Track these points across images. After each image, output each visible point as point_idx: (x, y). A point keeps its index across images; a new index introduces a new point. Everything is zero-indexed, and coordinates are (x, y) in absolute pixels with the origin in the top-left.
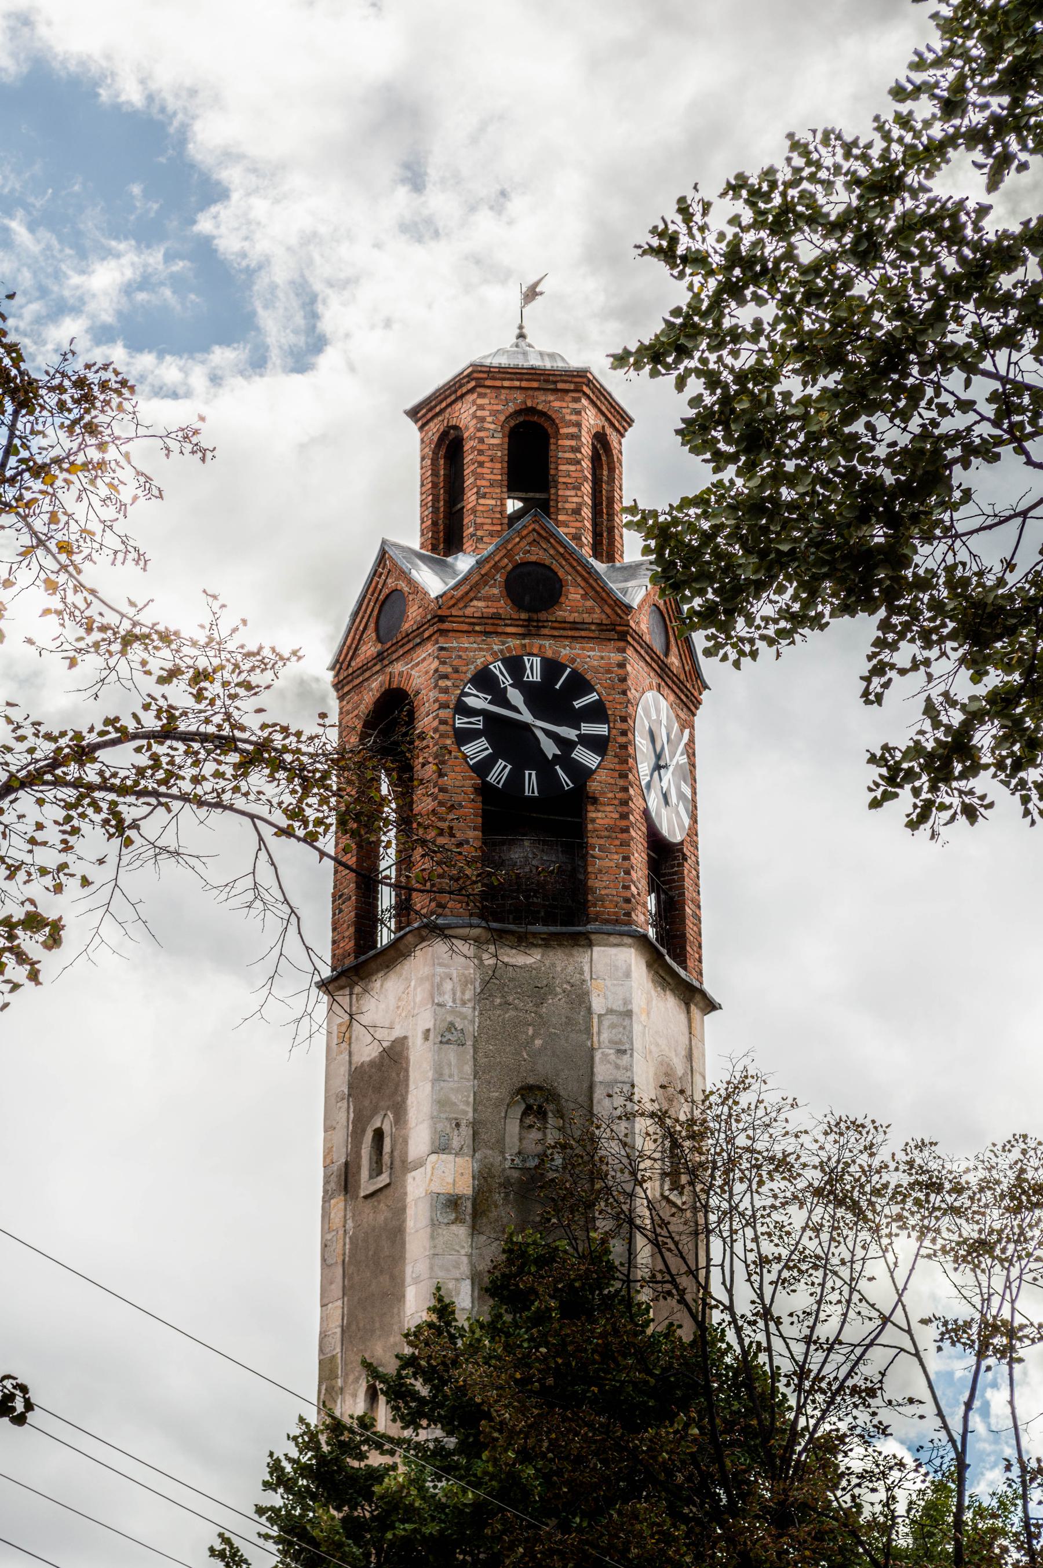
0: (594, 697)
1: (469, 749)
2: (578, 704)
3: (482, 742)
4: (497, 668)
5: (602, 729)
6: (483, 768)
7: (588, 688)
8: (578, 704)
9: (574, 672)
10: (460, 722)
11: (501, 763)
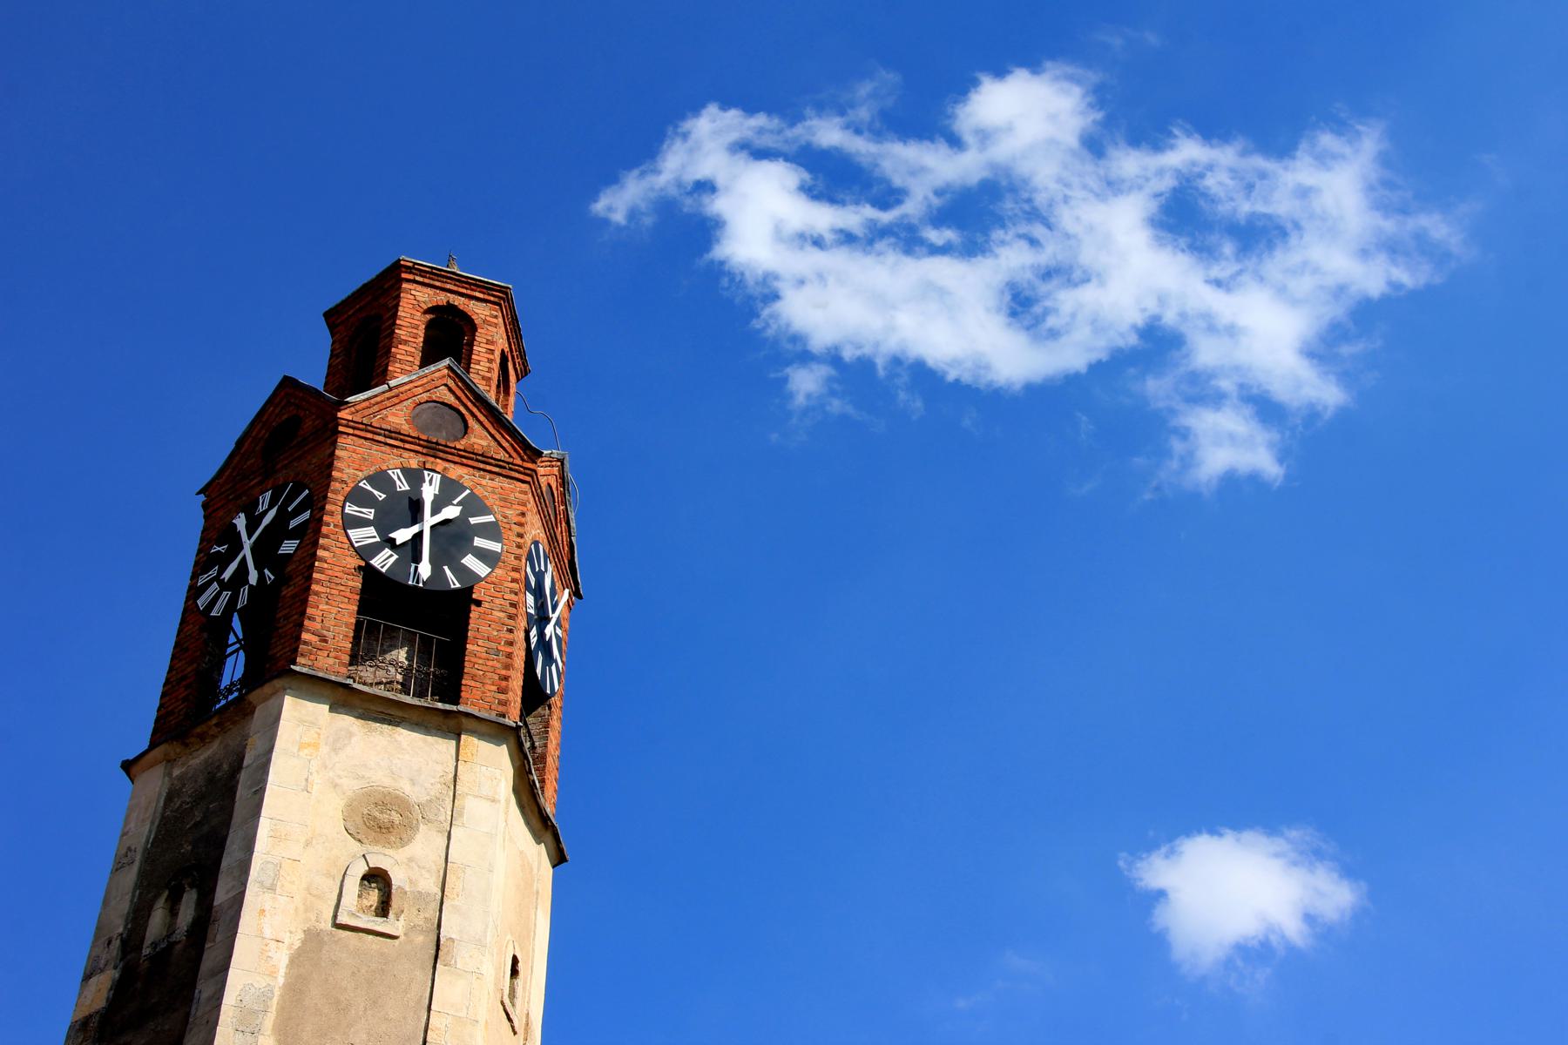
1: (355, 534)
2: (473, 521)
3: (371, 531)
4: (395, 474)
5: (495, 547)
6: (366, 552)
7: (485, 510)
8: (473, 521)
9: (472, 494)
10: (351, 509)
11: (387, 552)
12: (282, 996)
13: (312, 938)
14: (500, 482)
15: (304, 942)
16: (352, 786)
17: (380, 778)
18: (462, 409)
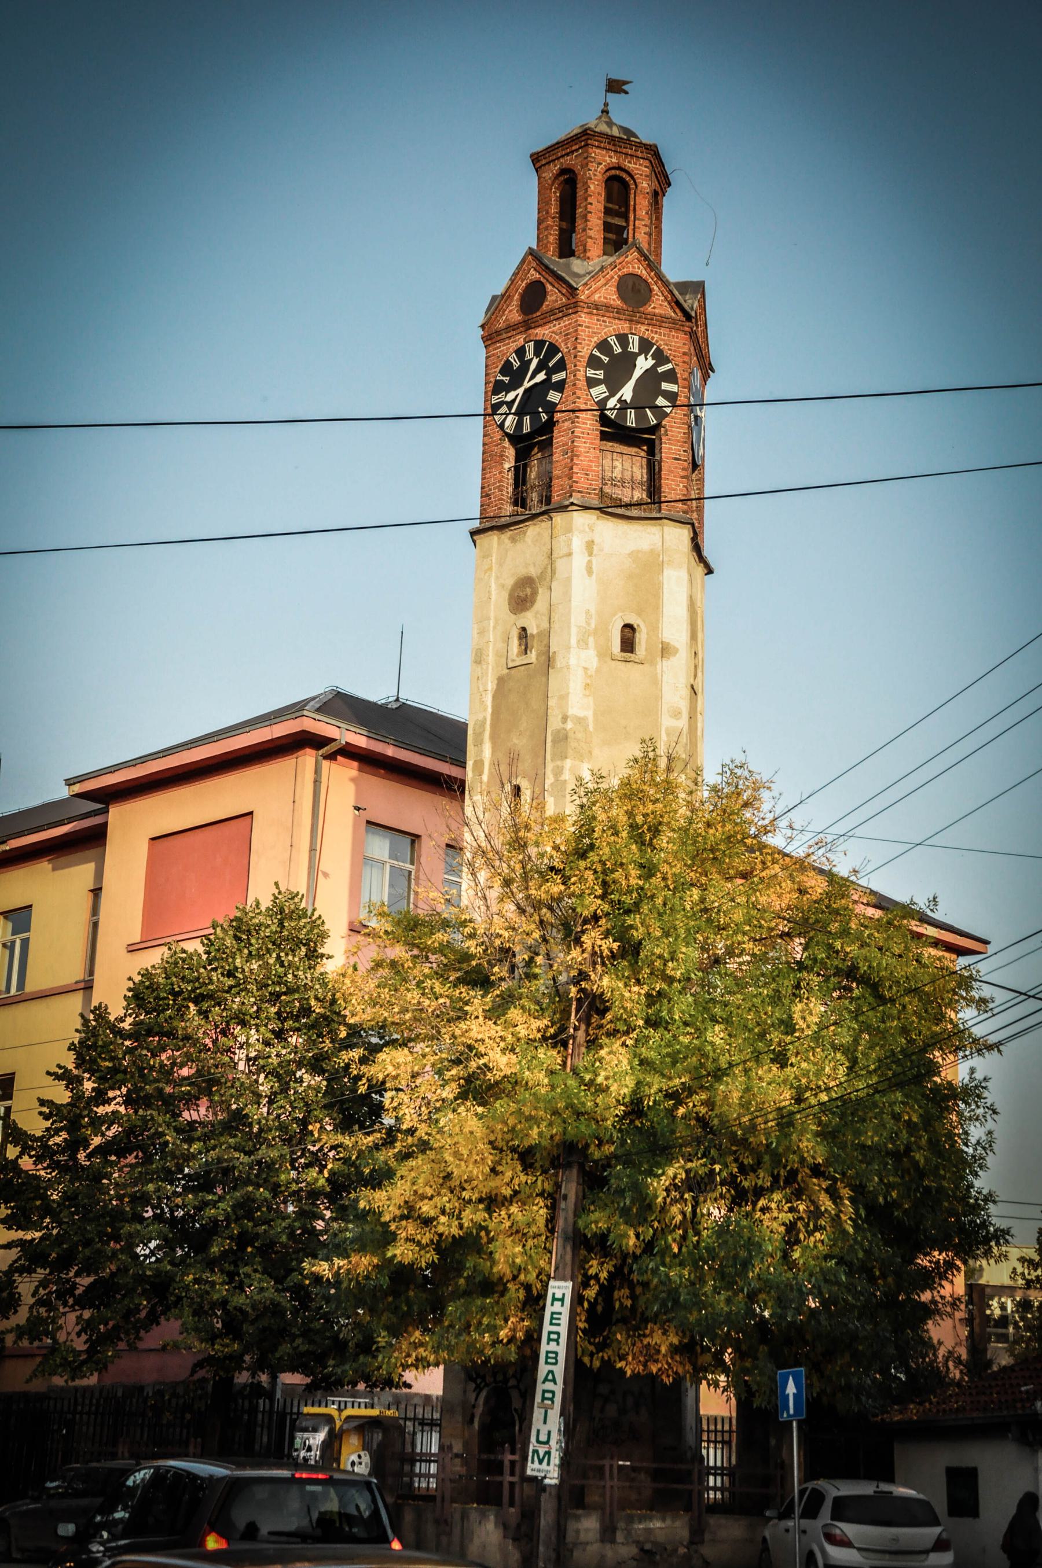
0: (560, 355)
12: (492, 719)
13: (501, 681)
14: (557, 326)
15: (498, 685)
16: (510, 582)
17: (522, 572)
18: (542, 279)
